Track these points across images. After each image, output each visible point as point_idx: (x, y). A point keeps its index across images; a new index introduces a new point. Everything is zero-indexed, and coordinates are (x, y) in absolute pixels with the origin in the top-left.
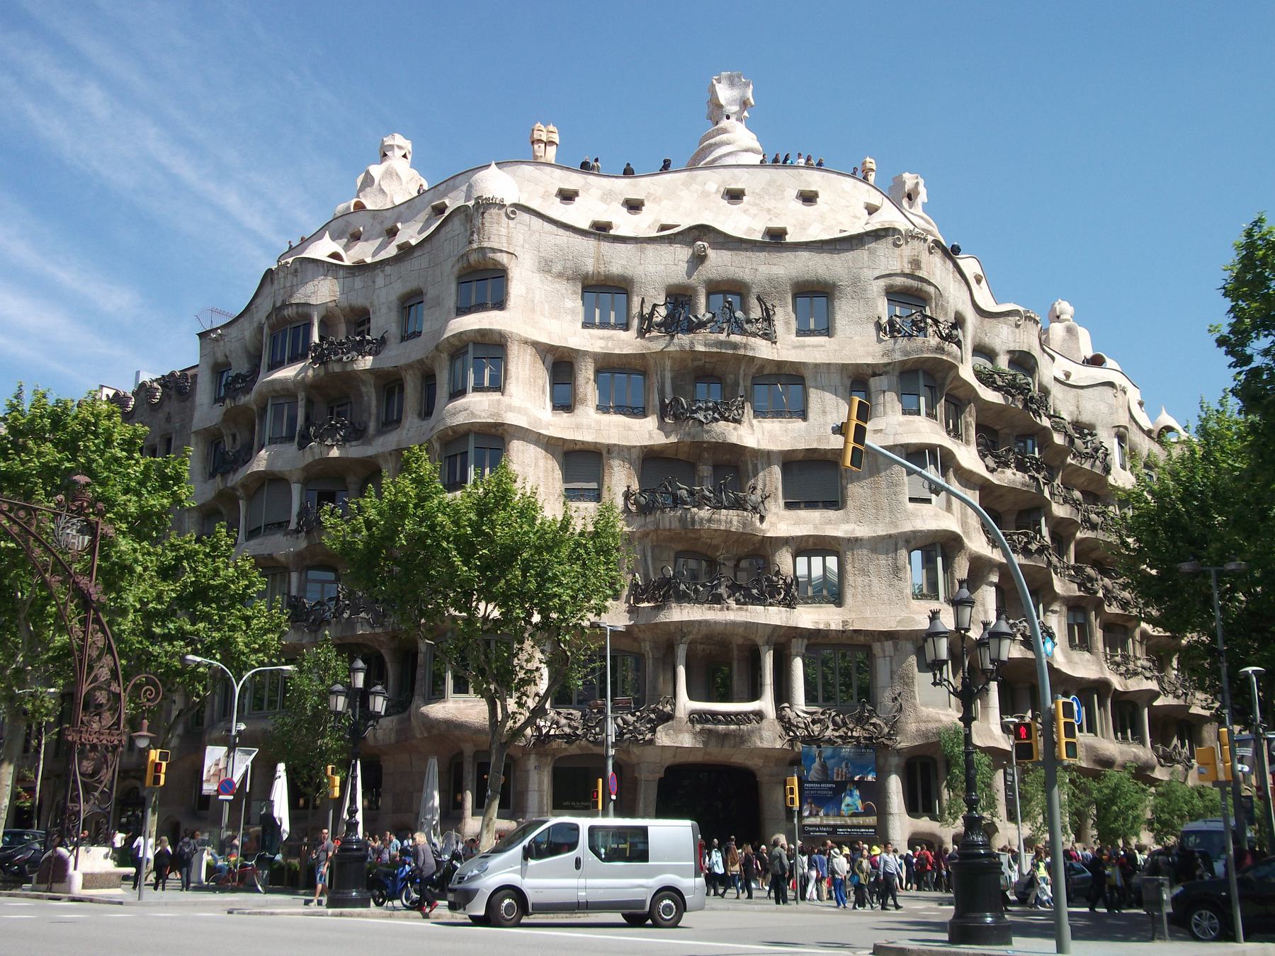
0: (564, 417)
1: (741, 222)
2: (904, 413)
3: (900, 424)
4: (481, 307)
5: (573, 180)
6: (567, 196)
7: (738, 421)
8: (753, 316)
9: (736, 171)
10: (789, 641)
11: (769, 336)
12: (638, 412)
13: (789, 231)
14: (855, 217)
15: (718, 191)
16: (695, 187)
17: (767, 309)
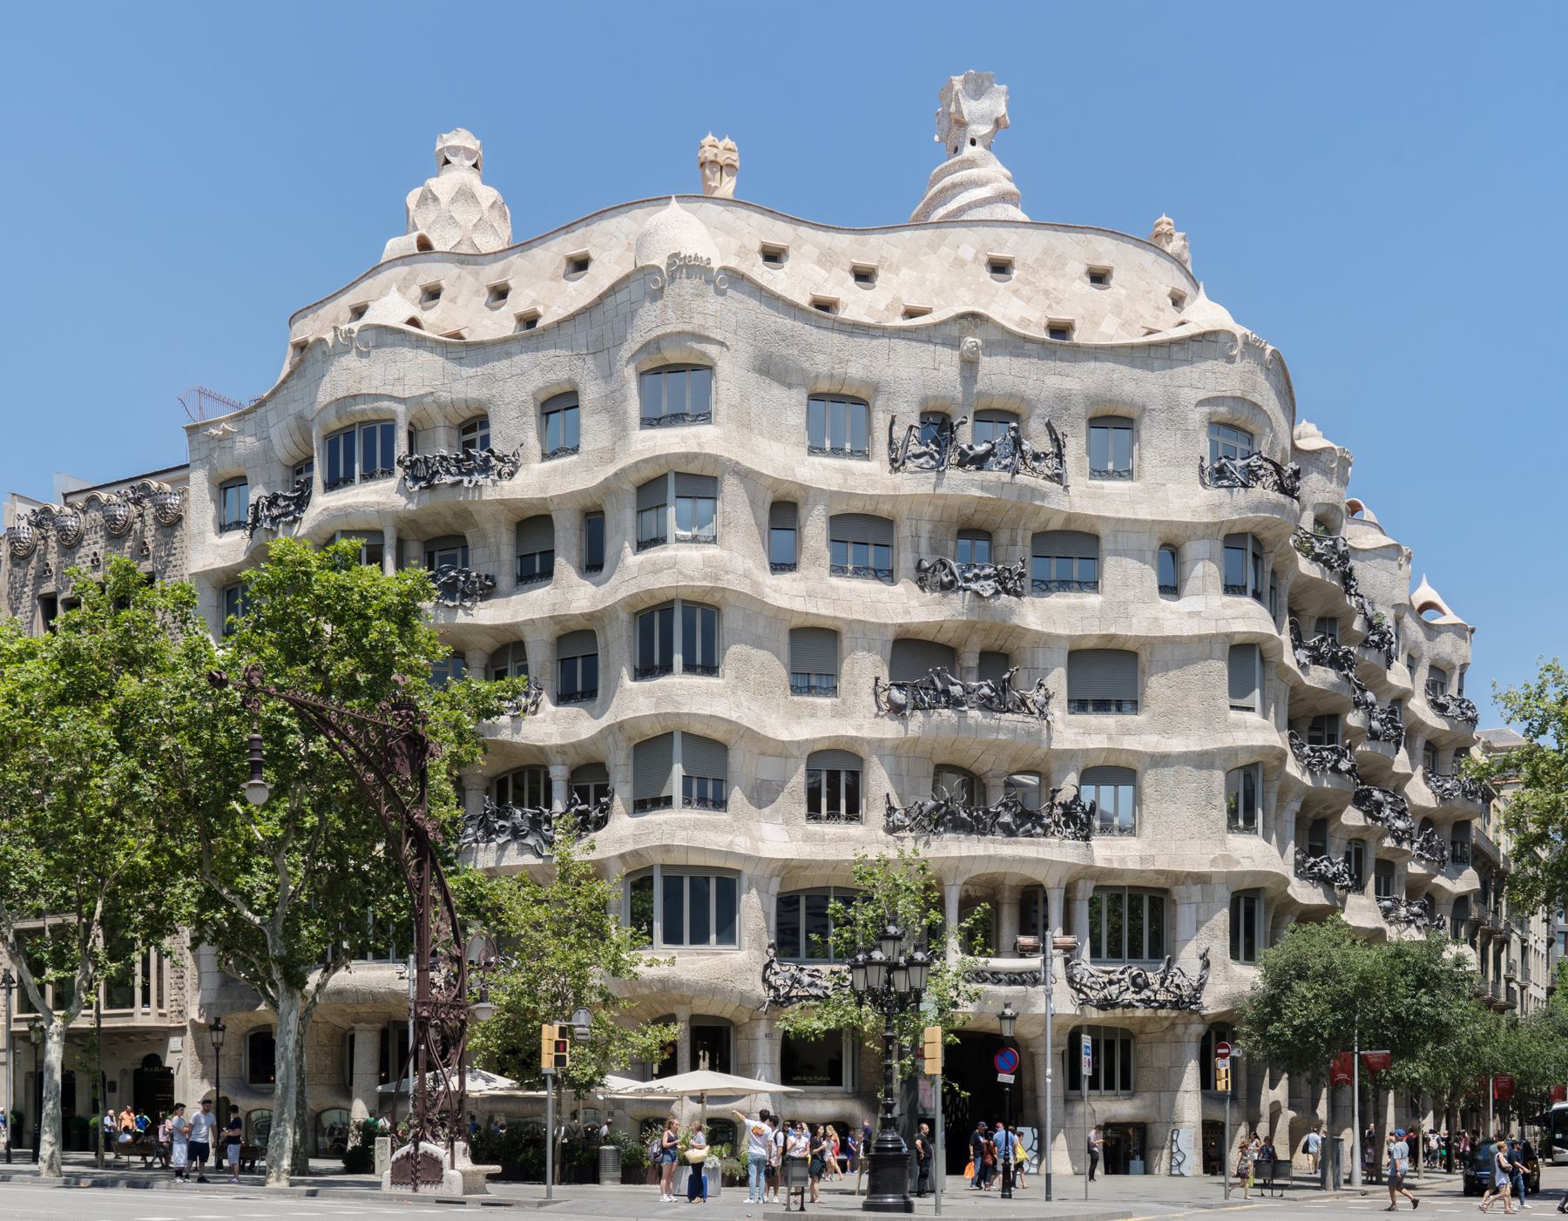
0: (785, 580)
1: (1015, 309)
2: (1231, 589)
3: (1224, 606)
4: (677, 418)
5: (778, 233)
6: (773, 256)
7: (1018, 595)
8: (1038, 450)
9: (1001, 231)
10: (1076, 882)
11: (1058, 478)
12: (886, 574)
13: (1077, 325)
14: (1158, 308)
15: (976, 258)
16: (944, 250)
17: (1057, 440)
